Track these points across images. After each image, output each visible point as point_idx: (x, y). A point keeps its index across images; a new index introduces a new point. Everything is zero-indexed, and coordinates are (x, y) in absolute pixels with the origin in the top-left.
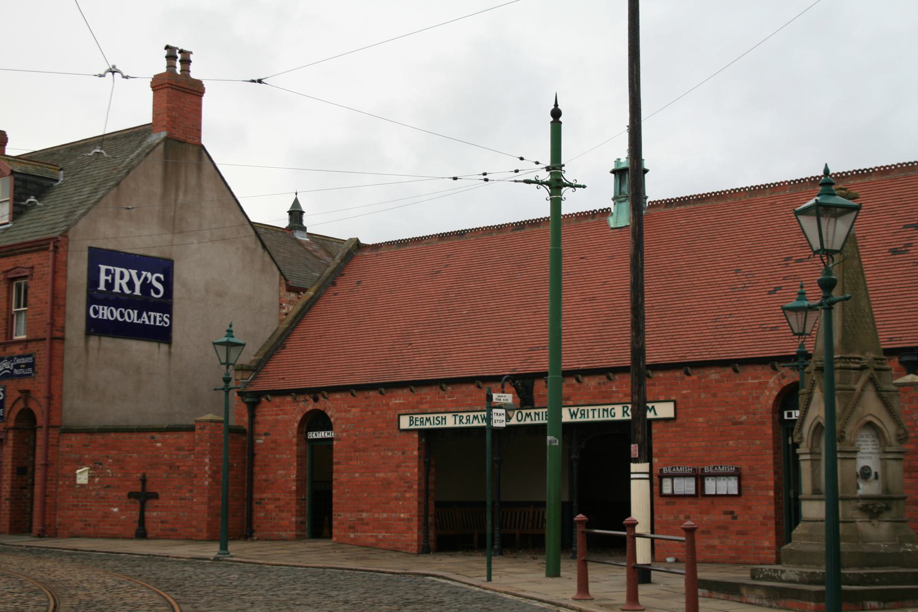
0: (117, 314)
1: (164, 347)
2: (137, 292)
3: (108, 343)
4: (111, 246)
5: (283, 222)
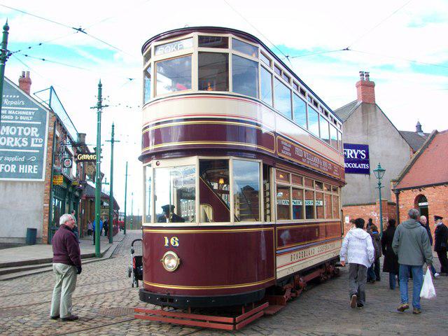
0: (349, 165)
1: (367, 176)
2: (356, 157)
5: (414, 130)
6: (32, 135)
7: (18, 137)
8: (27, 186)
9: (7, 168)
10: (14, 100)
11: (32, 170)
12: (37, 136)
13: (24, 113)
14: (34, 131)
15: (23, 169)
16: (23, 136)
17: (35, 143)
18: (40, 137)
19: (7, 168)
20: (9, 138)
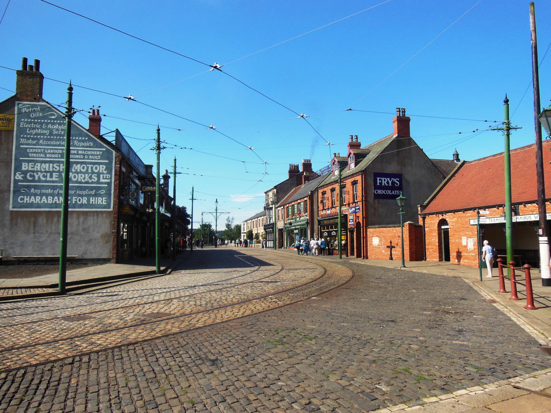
2: (390, 185)
3: (381, 201)
4: (381, 172)
6: (101, 171)
7: (88, 173)
8: (98, 216)
9: (80, 200)
10: (83, 141)
11: (102, 201)
12: (105, 172)
13: (93, 153)
14: (102, 168)
15: (94, 201)
16: (93, 173)
17: (103, 178)
18: (108, 173)
19: (80, 200)
20: (80, 175)
